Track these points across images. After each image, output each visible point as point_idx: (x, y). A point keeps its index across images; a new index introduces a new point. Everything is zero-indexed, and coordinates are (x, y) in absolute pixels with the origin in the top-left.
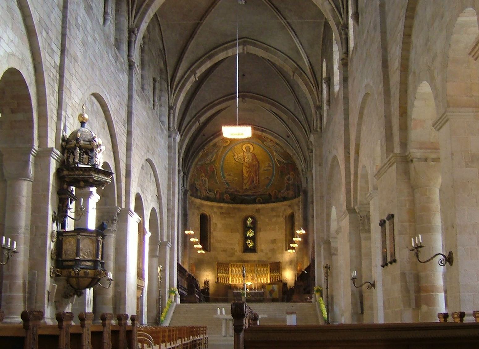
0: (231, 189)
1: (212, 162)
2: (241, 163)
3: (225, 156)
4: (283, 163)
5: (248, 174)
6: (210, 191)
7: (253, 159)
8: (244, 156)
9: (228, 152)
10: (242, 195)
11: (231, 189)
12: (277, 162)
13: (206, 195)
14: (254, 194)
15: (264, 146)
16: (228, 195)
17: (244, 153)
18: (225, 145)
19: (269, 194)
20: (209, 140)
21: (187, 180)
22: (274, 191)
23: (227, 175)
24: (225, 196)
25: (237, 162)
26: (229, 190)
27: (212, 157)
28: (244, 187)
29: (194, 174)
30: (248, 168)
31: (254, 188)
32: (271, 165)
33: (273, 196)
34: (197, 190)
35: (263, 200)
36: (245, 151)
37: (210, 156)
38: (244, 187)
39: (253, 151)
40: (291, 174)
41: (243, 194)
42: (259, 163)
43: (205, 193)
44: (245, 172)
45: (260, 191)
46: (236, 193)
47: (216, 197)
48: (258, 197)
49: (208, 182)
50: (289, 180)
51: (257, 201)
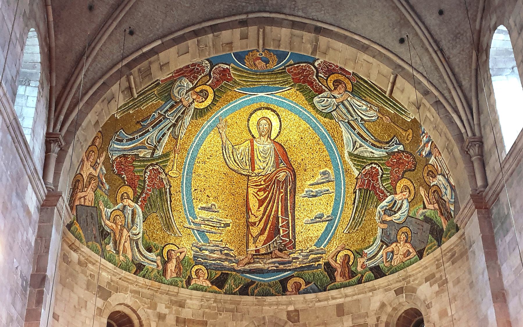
0: (212, 251)
1: (160, 157)
2: (242, 174)
3: (199, 145)
4: (372, 160)
5: (262, 209)
6: (149, 250)
7: (277, 164)
8: (253, 150)
9: (207, 133)
10: (244, 272)
11: (212, 251)
12: (351, 163)
13: (133, 255)
14: (281, 267)
15: (313, 112)
16: (203, 268)
17: (252, 143)
18: (195, 105)
19: (327, 264)
20: (145, 50)
21: (59, 161)
22: (340, 254)
23: (203, 208)
24: (194, 269)
25: (231, 169)
26: (207, 253)
27: (159, 142)
28: (252, 248)
29: (94, 173)
30: (264, 190)
31: (281, 250)
32: (332, 177)
33: (339, 270)
34: (104, 234)
35: (307, 283)
36: (257, 135)
37: (153, 134)
38: (252, 248)
39: (279, 132)
40: (398, 190)
41: (247, 267)
42: (293, 170)
43: (132, 250)
44: (253, 203)
45: (297, 258)
46: (226, 263)
47: (165, 270)
48: (293, 276)
49: (145, 219)
50: (391, 210)
51: (290, 289)
